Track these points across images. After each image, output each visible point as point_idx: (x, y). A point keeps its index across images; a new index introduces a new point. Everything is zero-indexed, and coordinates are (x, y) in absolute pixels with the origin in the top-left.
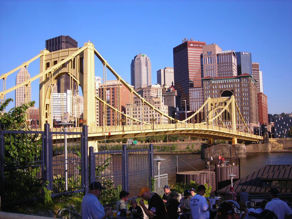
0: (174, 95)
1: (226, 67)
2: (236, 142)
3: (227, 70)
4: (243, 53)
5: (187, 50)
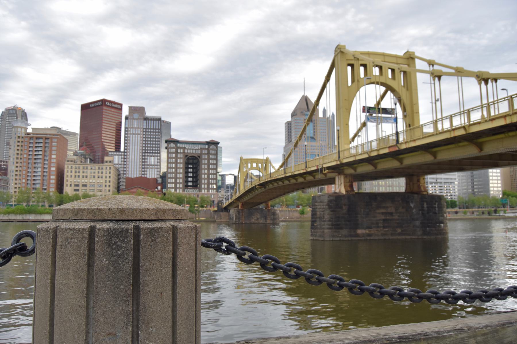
0: (87, 158)
4: (165, 122)
5: (103, 109)
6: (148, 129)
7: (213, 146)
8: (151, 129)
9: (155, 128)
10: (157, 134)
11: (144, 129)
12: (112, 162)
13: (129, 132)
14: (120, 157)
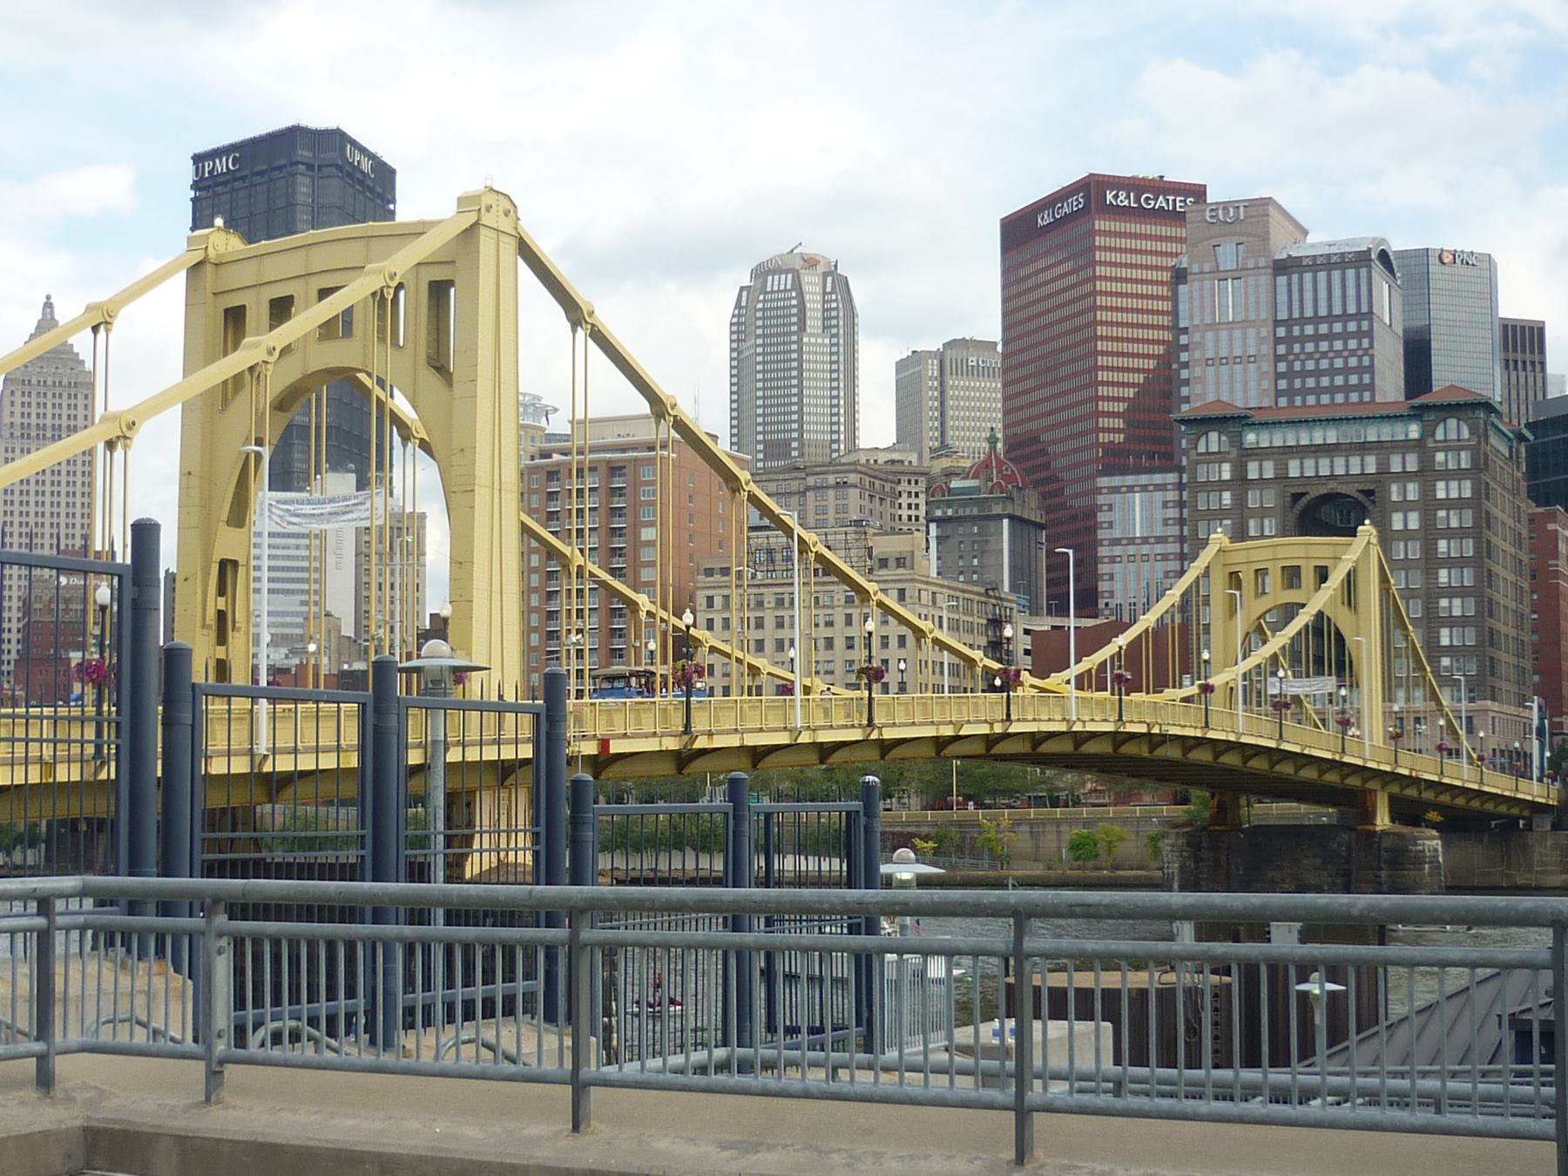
0: (1000, 517)
2: (1383, 821)
4: (1448, 258)
6: (1302, 321)
7: (1452, 423)
8: (1316, 320)
10: (1353, 344)
11: (1277, 323)
12: (908, 564)
13: (1197, 355)
14: (1158, 496)
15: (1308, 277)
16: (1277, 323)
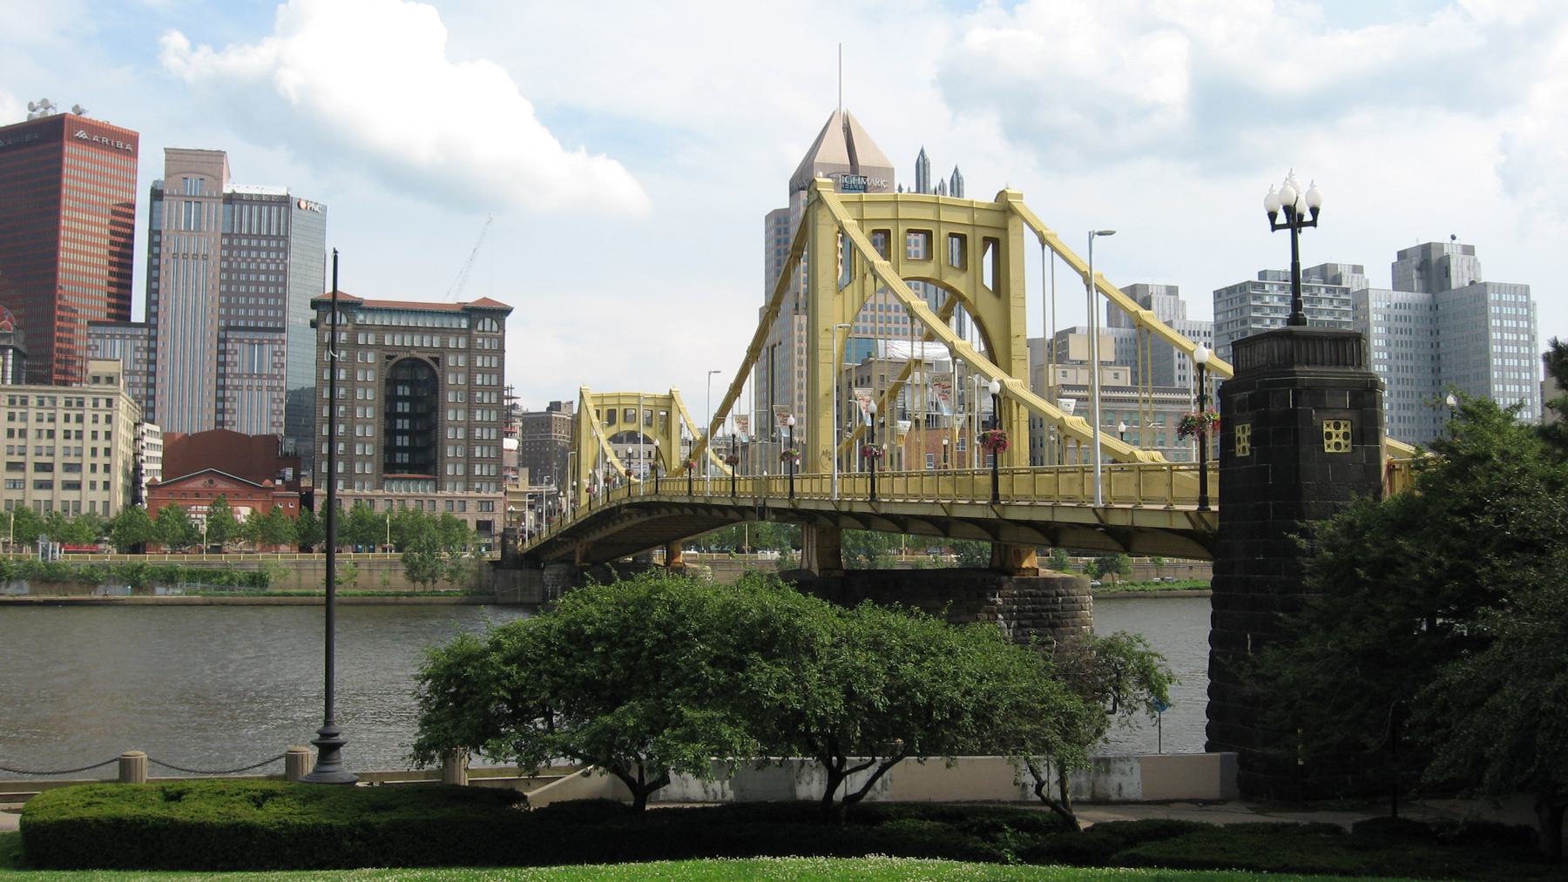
1: (263, 255)
3: (263, 266)
4: (303, 205)
7: (488, 321)
8: (249, 236)
9: (264, 232)
12: (115, 381)
15: (246, 208)
16: (224, 235)
